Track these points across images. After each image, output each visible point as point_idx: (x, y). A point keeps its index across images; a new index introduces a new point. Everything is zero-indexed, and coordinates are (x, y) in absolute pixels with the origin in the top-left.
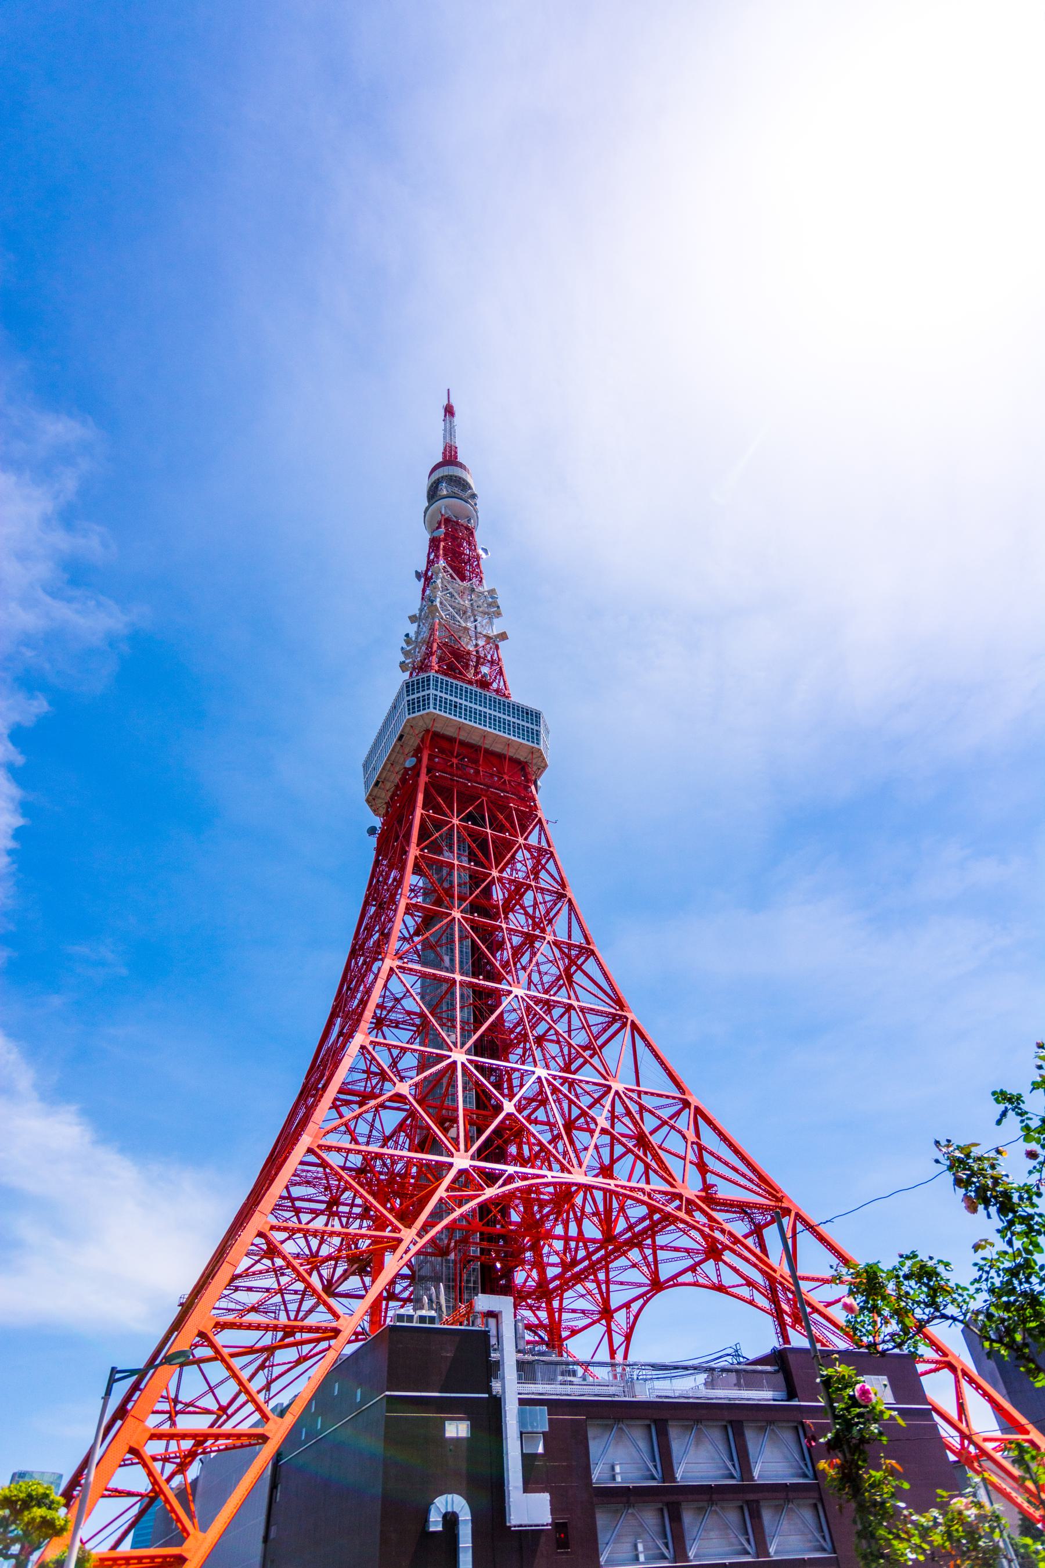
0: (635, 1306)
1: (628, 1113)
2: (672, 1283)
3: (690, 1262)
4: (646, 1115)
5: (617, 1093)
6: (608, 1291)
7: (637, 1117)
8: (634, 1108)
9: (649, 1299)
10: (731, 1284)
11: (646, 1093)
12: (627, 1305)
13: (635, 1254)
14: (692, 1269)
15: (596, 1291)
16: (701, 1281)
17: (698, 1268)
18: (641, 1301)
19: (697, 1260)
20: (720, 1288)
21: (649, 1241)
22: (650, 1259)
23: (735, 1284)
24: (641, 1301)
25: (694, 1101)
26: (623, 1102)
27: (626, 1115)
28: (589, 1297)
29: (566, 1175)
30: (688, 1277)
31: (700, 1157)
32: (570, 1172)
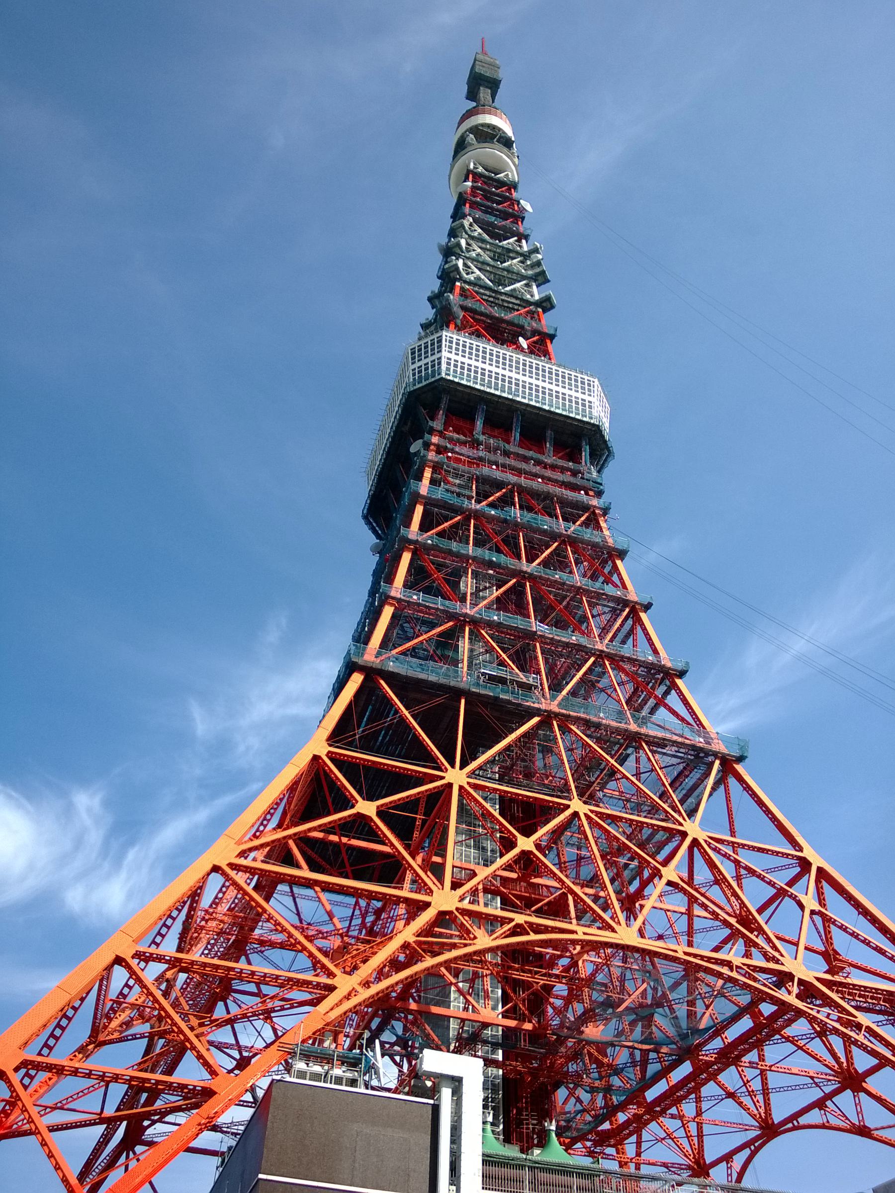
0: (739, 1160)
1: (719, 880)
2: (790, 1125)
3: (817, 1094)
4: (750, 882)
5: (695, 842)
6: (700, 1136)
7: (734, 884)
8: (727, 870)
9: (757, 1150)
10: (879, 1126)
11: (743, 846)
12: (727, 1158)
13: (730, 1077)
14: (820, 1104)
15: (681, 1133)
16: (834, 1121)
17: (829, 1103)
18: (746, 1153)
19: (828, 1089)
20: (863, 1131)
21: (753, 1056)
22: (756, 1085)
23: (885, 1125)
24: (746, 1153)
25: (817, 861)
26: (704, 854)
27: (717, 882)
28: (670, 1141)
29: (607, 933)
30: (815, 1117)
31: (828, 939)
32: (614, 931)
